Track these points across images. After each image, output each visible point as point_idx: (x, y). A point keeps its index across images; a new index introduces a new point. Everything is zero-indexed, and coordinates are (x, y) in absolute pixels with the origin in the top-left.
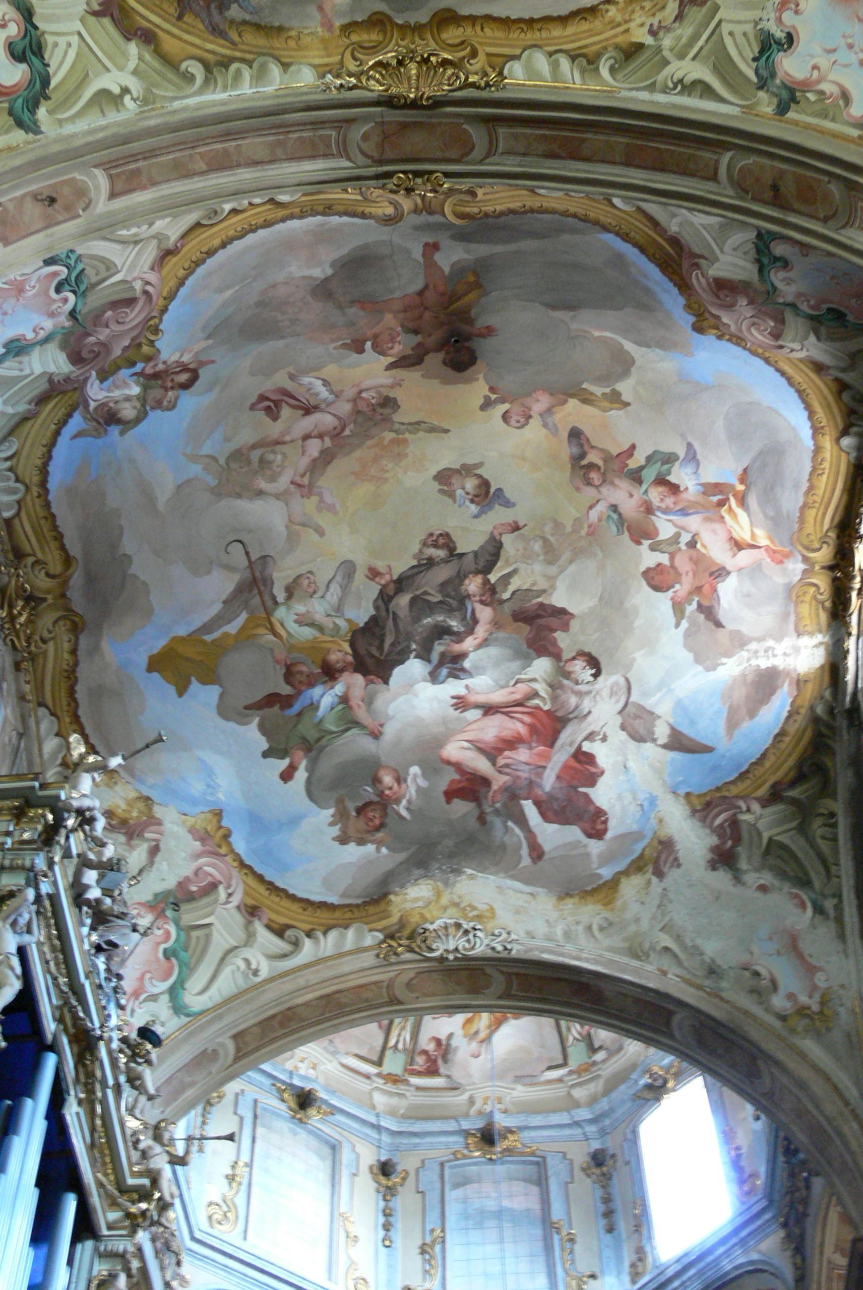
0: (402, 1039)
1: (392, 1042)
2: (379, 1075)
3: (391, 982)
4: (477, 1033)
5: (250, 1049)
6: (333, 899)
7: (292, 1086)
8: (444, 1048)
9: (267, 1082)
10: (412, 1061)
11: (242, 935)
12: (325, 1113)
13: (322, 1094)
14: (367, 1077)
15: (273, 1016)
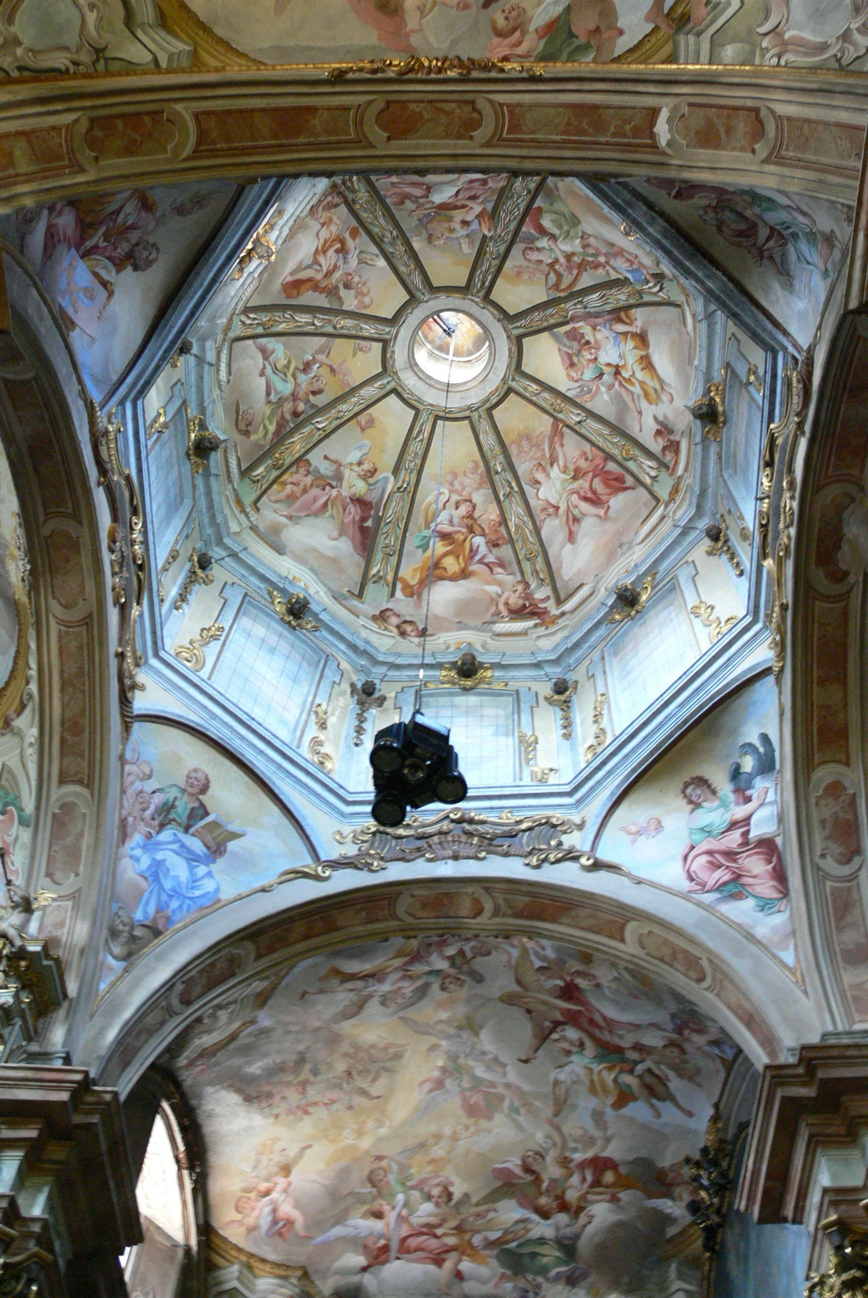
0: (648, 470)
1: (648, 481)
2: (666, 506)
3: (61, 622)
4: (655, 390)
5: (86, 772)
6: (13, 650)
7: (612, 607)
8: (664, 429)
9: (602, 631)
10: (666, 467)
11: (17, 739)
12: (653, 579)
13: (629, 581)
14: (663, 518)
15: (63, 741)
